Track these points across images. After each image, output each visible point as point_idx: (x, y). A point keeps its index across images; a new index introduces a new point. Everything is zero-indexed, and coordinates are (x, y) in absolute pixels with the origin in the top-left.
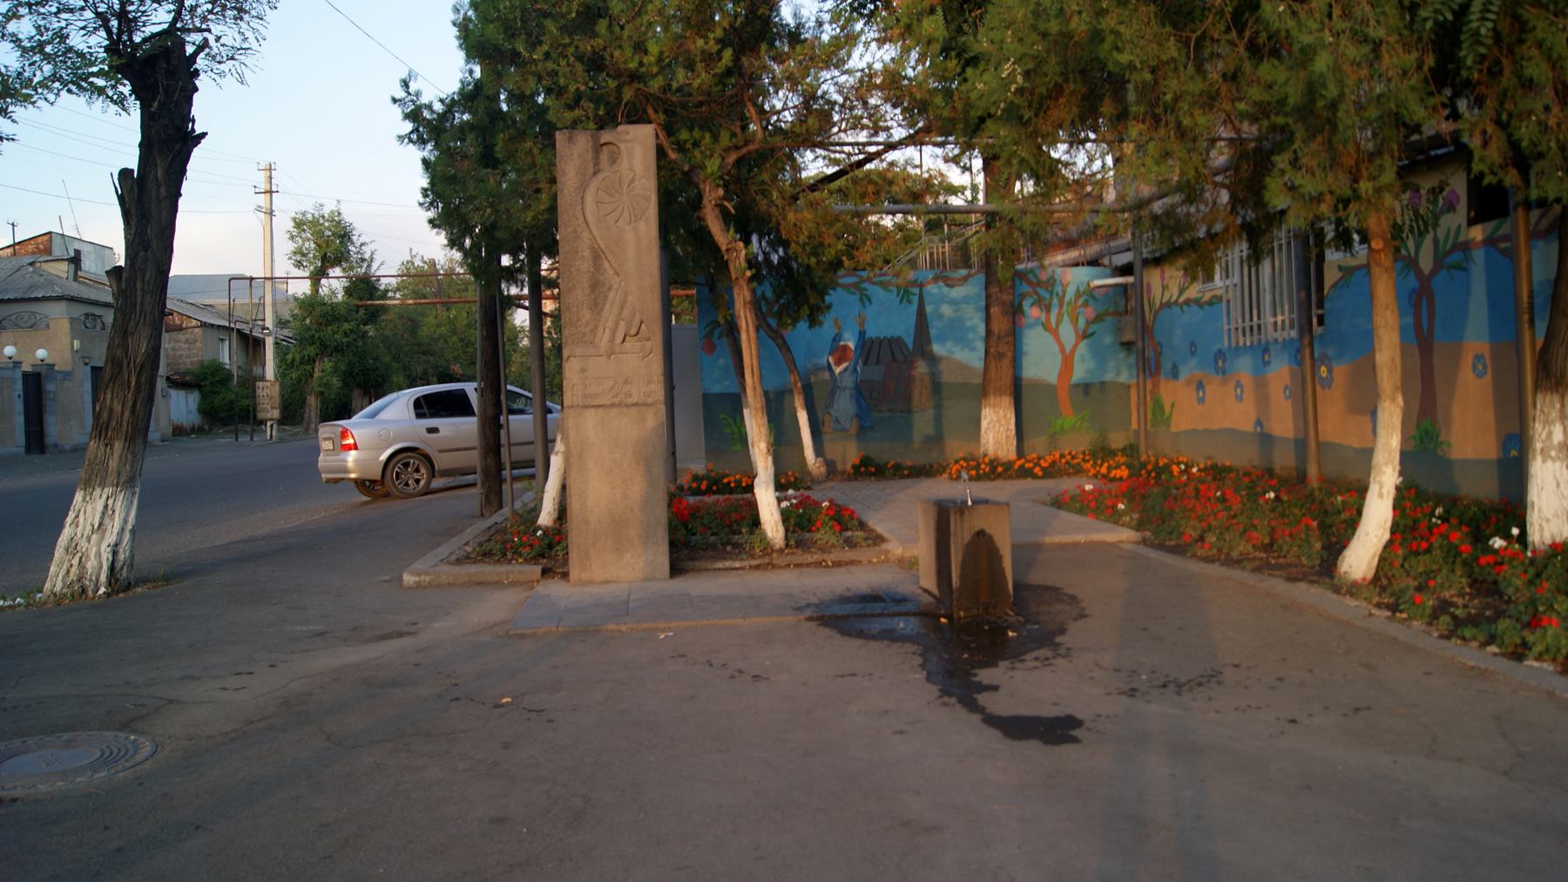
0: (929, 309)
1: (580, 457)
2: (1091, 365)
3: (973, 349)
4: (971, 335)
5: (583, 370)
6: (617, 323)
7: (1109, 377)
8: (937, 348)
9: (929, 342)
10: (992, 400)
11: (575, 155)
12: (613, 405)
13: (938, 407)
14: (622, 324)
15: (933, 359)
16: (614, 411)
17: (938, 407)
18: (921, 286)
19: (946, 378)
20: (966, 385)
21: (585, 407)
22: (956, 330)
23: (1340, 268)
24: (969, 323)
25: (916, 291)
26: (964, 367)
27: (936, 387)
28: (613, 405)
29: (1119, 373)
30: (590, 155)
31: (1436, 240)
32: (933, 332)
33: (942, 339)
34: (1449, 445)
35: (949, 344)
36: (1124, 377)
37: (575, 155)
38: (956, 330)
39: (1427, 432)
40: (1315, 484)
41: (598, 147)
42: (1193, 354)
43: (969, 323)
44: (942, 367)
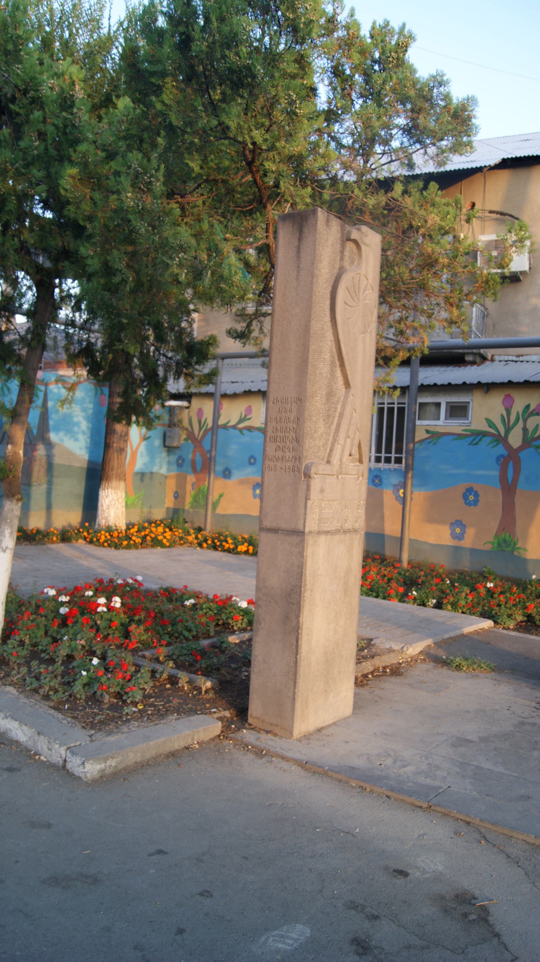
0: (50, 404)
1: (312, 591)
2: (146, 459)
3: (77, 440)
4: (76, 429)
5: (322, 491)
6: (345, 440)
7: (155, 469)
8: (53, 437)
9: (48, 431)
10: (114, 483)
11: (330, 242)
12: (337, 532)
13: (50, 483)
14: (348, 440)
15: (49, 445)
16: (337, 538)
17: (50, 483)
18: (46, 385)
19: (57, 460)
20: (70, 466)
21: (319, 533)
22: (67, 425)
23: (427, 431)
24: (75, 420)
25: (43, 388)
26: (70, 453)
27: (50, 466)
28: (337, 532)
29: (161, 467)
30: (338, 247)
31: (525, 430)
32: (51, 423)
33: (57, 429)
34: (526, 550)
35: (61, 434)
36: (164, 471)
37: (330, 242)
38: (67, 425)
39: (505, 541)
40: (405, 564)
41: (347, 239)
42: (250, 464)
43: (75, 420)
44: (55, 451)
